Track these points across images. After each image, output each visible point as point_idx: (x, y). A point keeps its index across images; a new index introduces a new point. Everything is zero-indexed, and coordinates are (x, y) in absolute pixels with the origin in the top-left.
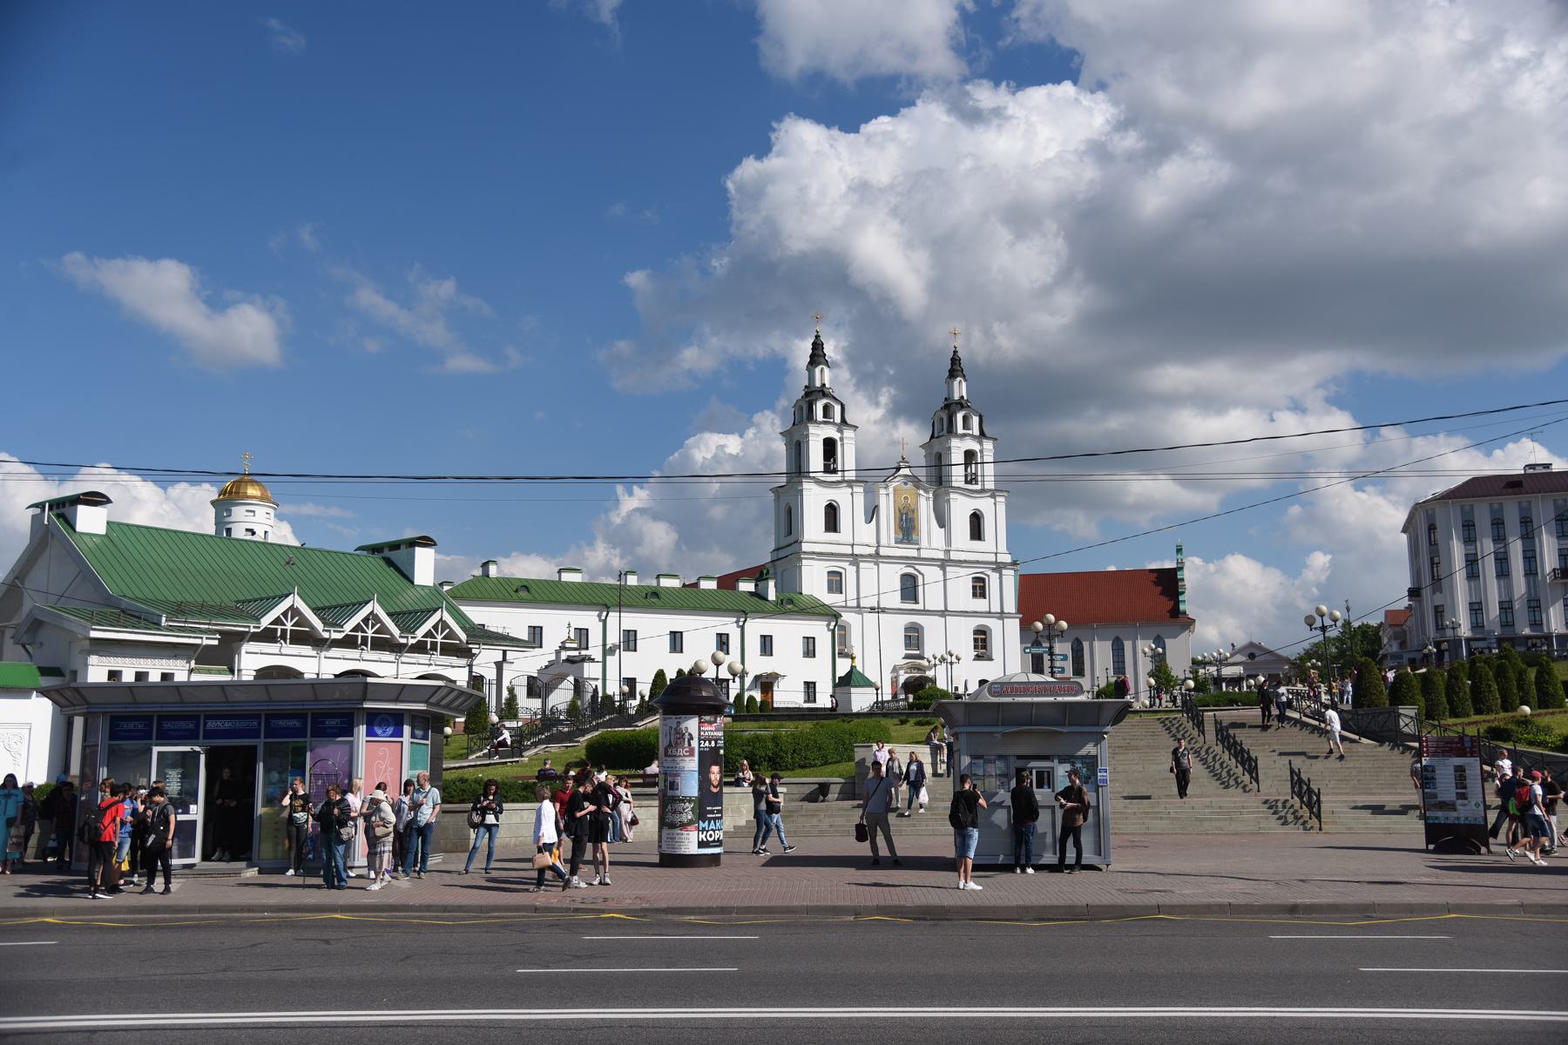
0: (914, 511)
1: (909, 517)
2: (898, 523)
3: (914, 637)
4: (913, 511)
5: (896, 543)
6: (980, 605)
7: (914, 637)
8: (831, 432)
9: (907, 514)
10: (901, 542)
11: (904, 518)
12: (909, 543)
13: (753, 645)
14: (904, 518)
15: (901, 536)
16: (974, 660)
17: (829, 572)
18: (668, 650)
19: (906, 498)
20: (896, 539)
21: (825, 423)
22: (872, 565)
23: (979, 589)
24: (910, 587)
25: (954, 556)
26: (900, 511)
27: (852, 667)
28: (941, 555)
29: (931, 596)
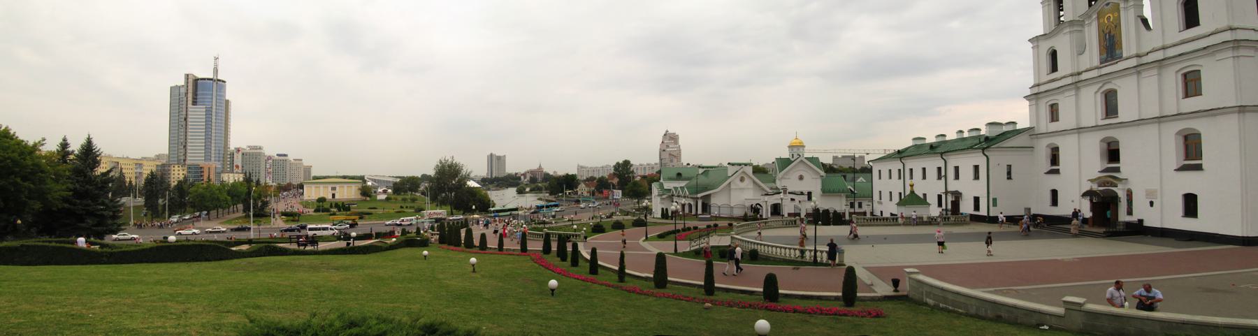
0: (1118, 25)
1: (1112, 34)
2: (1102, 41)
3: (1113, 154)
4: (1116, 26)
5: (1101, 63)
7: (1113, 154)
9: (1110, 32)
10: (1106, 61)
11: (1107, 37)
15: (1105, 56)
22: (1073, 92)
23: (1191, 84)
24: (1110, 105)
26: (1103, 31)
27: (912, 192)
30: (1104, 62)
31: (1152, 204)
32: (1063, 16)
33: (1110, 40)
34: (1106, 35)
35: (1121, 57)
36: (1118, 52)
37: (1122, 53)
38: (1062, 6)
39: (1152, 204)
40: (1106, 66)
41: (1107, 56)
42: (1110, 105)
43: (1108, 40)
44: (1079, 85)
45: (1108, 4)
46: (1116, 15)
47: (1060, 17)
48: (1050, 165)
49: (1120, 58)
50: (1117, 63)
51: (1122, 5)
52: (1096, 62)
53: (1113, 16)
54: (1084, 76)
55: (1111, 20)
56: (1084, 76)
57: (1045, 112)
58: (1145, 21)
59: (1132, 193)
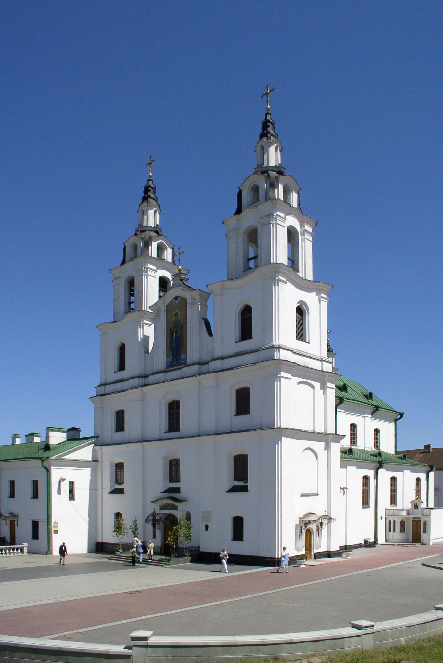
5: (167, 367)
9: (176, 332)
10: (172, 365)
11: (174, 337)
12: (178, 364)
14: (174, 337)
15: (171, 359)
16: (227, 492)
20: (167, 362)
26: (171, 331)
31: (207, 527)
32: (133, 302)
33: (176, 344)
34: (172, 335)
35: (185, 363)
36: (182, 356)
37: (186, 359)
38: (133, 290)
39: (207, 527)
40: (171, 371)
41: (173, 360)
43: (174, 341)
47: (130, 303)
49: (186, 365)
50: (181, 368)
54: (151, 379)
55: (178, 318)
58: (208, 325)
59: (190, 516)
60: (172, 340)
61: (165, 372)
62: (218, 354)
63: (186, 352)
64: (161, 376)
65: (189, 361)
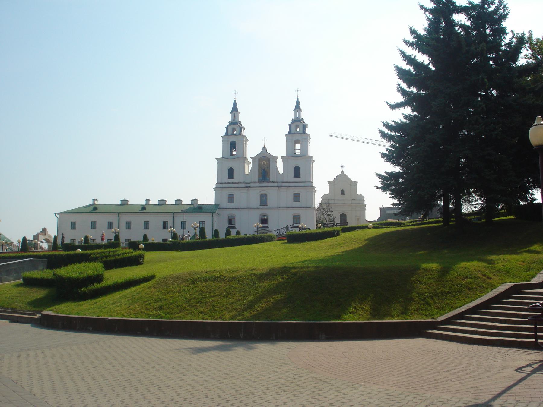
0: (268, 167)
4: (267, 168)
6: (297, 204)
8: (233, 139)
9: (264, 169)
10: (261, 181)
11: (263, 171)
13: (178, 224)
15: (261, 178)
17: (228, 195)
18: (162, 228)
19: (264, 163)
21: (231, 135)
23: (297, 198)
24: (264, 200)
25: (284, 184)
28: (280, 184)
29: (272, 201)
30: (260, 181)
34: (262, 170)
35: (269, 181)
36: (267, 178)
41: (262, 179)
42: (264, 200)
44: (250, 188)
45: (264, 157)
46: (268, 163)
48: (228, 224)
49: (268, 181)
51: (271, 159)
52: (257, 181)
53: (267, 163)
54: (252, 185)
56: (252, 185)
57: (226, 199)
60: (262, 171)
61: (258, 183)
62: (286, 180)
63: (269, 177)
64: (257, 185)
65: (271, 180)
